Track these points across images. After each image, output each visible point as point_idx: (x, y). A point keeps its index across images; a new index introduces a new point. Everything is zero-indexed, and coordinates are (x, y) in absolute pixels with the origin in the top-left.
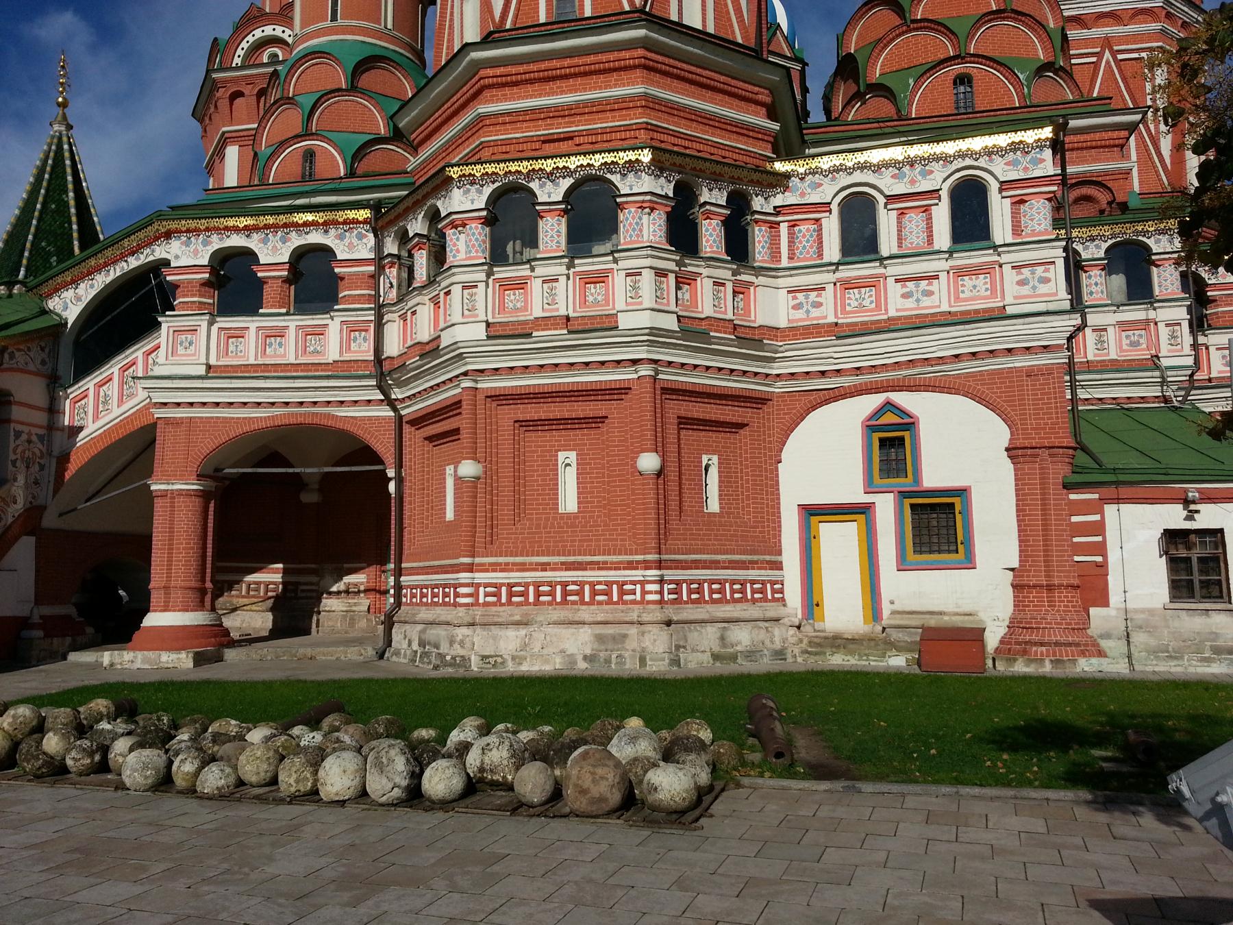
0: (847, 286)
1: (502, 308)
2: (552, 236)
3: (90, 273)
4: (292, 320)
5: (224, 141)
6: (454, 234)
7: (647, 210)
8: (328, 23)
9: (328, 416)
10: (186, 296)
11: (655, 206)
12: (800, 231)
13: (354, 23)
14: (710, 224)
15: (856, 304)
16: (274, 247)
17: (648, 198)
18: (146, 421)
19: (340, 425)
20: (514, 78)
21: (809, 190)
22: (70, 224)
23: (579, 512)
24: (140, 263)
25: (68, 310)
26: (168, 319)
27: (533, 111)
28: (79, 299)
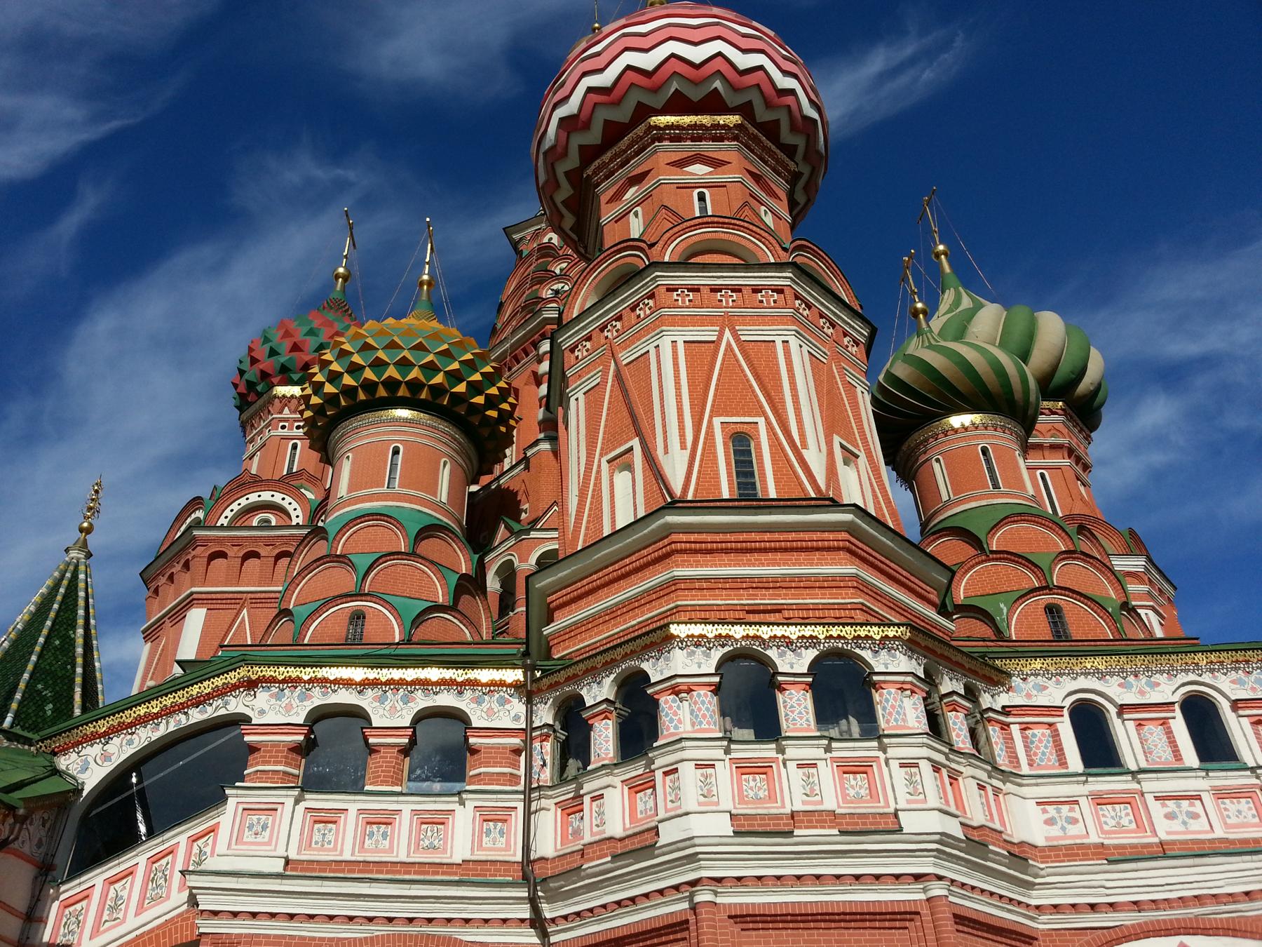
0: (1099, 801)
1: (742, 799)
2: (800, 713)
3: (131, 725)
4: (407, 802)
5: (190, 602)
6: (674, 701)
7: (908, 692)
8: (384, 489)
10: (268, 763)
11: (916, 689)
12: (1035, 735)
13: (412, 492)
14: (957, 717)
16: (393, 708)
17: (909, 679)
18: (187, 937)
20: (709, 546)
21: (1035, 692)
22: (74, 667)
24: (205, 716)
25: (89, 772)
26: (240, 792)
27: (734, 579)
28: (106, 757)
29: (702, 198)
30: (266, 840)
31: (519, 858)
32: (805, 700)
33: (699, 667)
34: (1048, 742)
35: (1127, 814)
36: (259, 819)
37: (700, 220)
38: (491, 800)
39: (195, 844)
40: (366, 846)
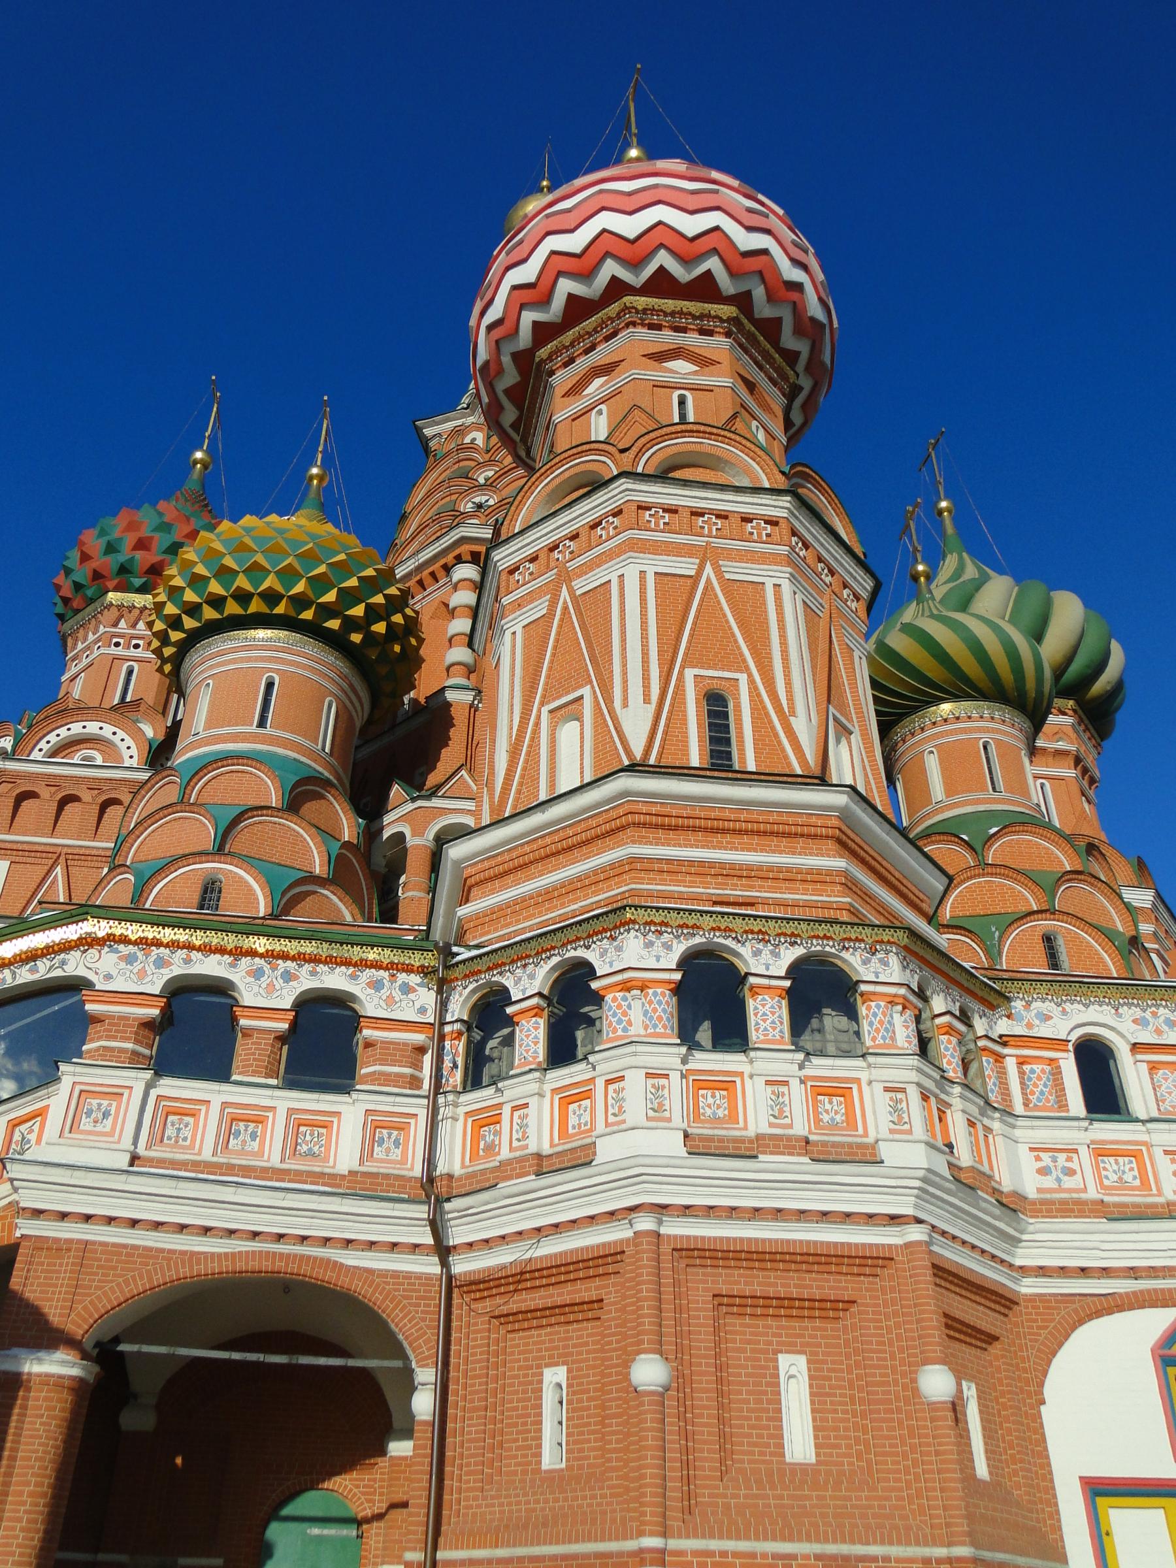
1: (697, 1115)
9: (327, 1263)
10: (114, 1038)
12: (1032, 1071)
13: (287, 735)
14: (949, 1042)
15: (1115, 1178)
19: (344, 1282)
21: (1037, 1022)
23: (818, 1462)
24: (36, 977)
29: (682, 402)
30: (108, 1129)
31: (417, 1170)
32: (780, 1008)
33: (658, 961)
34: (1048, 1079)
35: (1131, 1169)
36: (100, 1105)
37: (679, 428)
38: (387, 1103)
39: (17, 1130)
40: (230, 1146)
